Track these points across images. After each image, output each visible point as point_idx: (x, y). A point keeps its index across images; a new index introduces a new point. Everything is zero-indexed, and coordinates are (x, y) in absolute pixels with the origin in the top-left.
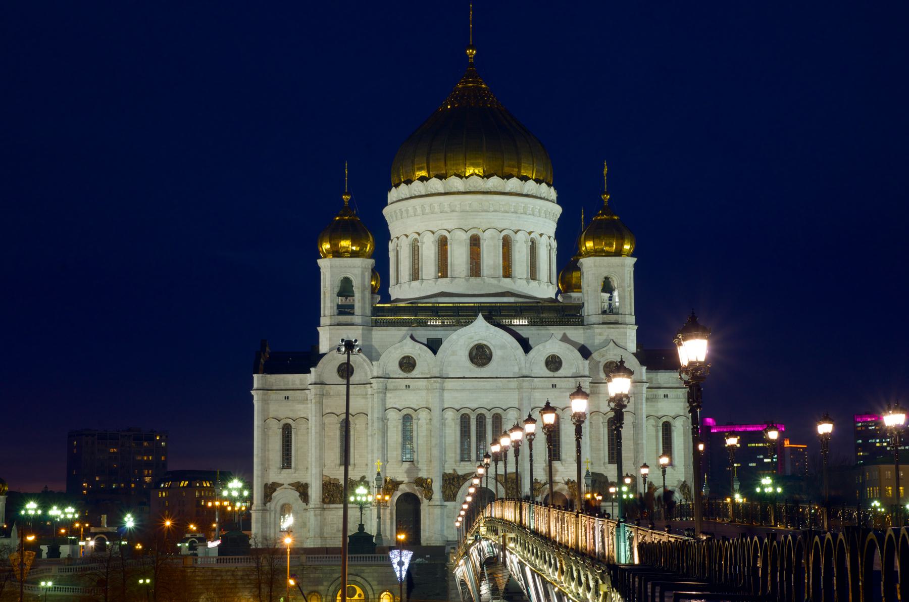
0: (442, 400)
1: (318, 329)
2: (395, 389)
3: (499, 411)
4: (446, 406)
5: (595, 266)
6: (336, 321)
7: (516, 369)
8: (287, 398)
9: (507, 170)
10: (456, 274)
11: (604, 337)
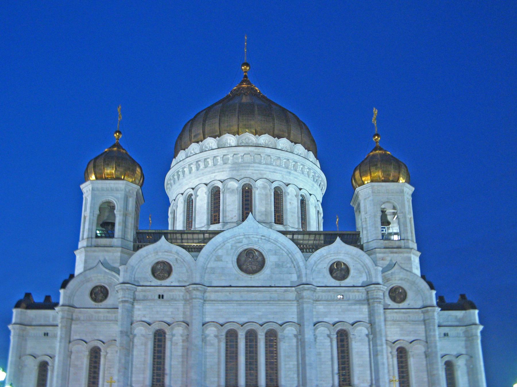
0: (203, 314)
1: (76, 252)
2: (145, 299)
3: (274, 327)
4: (207, 320)
5: (373, 192)
6: (93, 243)
7: (294, 277)
8: (46, 334)
9: (276, 132)
10: (228, 219)
11: (387, 262)
